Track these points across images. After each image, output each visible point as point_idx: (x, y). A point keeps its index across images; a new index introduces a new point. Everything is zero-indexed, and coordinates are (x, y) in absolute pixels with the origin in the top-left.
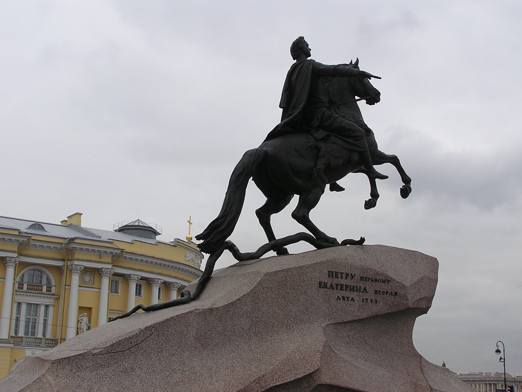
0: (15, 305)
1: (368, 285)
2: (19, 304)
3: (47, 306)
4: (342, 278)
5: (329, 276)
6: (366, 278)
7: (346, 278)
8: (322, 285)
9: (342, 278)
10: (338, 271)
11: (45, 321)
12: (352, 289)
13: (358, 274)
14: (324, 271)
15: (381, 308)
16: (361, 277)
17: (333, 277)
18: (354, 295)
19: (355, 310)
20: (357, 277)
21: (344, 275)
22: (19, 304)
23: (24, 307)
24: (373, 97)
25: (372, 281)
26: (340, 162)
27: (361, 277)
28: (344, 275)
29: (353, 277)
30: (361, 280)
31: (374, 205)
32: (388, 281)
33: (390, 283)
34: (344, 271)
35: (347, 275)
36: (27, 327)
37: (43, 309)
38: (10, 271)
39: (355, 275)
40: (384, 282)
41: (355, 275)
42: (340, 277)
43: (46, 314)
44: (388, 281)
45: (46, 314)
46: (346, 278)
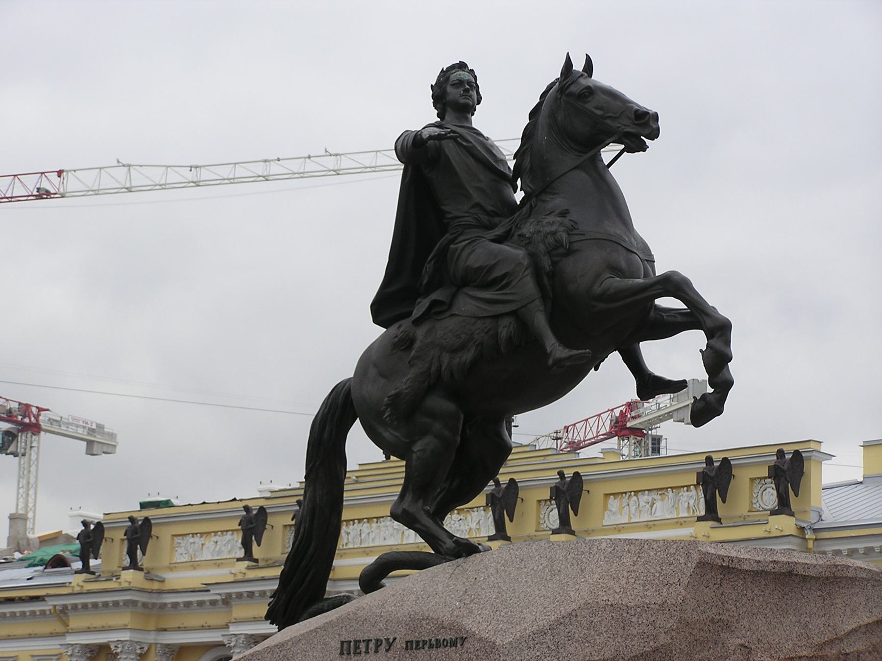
4: (367, 652)
5: (342, 653)
6: (418, 642)
7: (376, 651)
9: (367, 652)
10: (360, 636)
13: (401, 635)
14: (333, 643)
16: (407, 642)
17: (349, 654)
20: (399, 644)
21: (372, 645)
24: (637, 128)
25: (431, 647)
26: (468, 356)
27: (407, 642)
28: (372, 645)
29: (390, 645)
30: (407, 649)
31: (718, 411)
32: (463, 640)
33: (466, 645)
34: (373, 635)
35: (378, 643)
39: (395, 639)
40: (453, 643)
41: (395, 639)
42: (363, 650)
44: (463, 640)
46: (376, 651)
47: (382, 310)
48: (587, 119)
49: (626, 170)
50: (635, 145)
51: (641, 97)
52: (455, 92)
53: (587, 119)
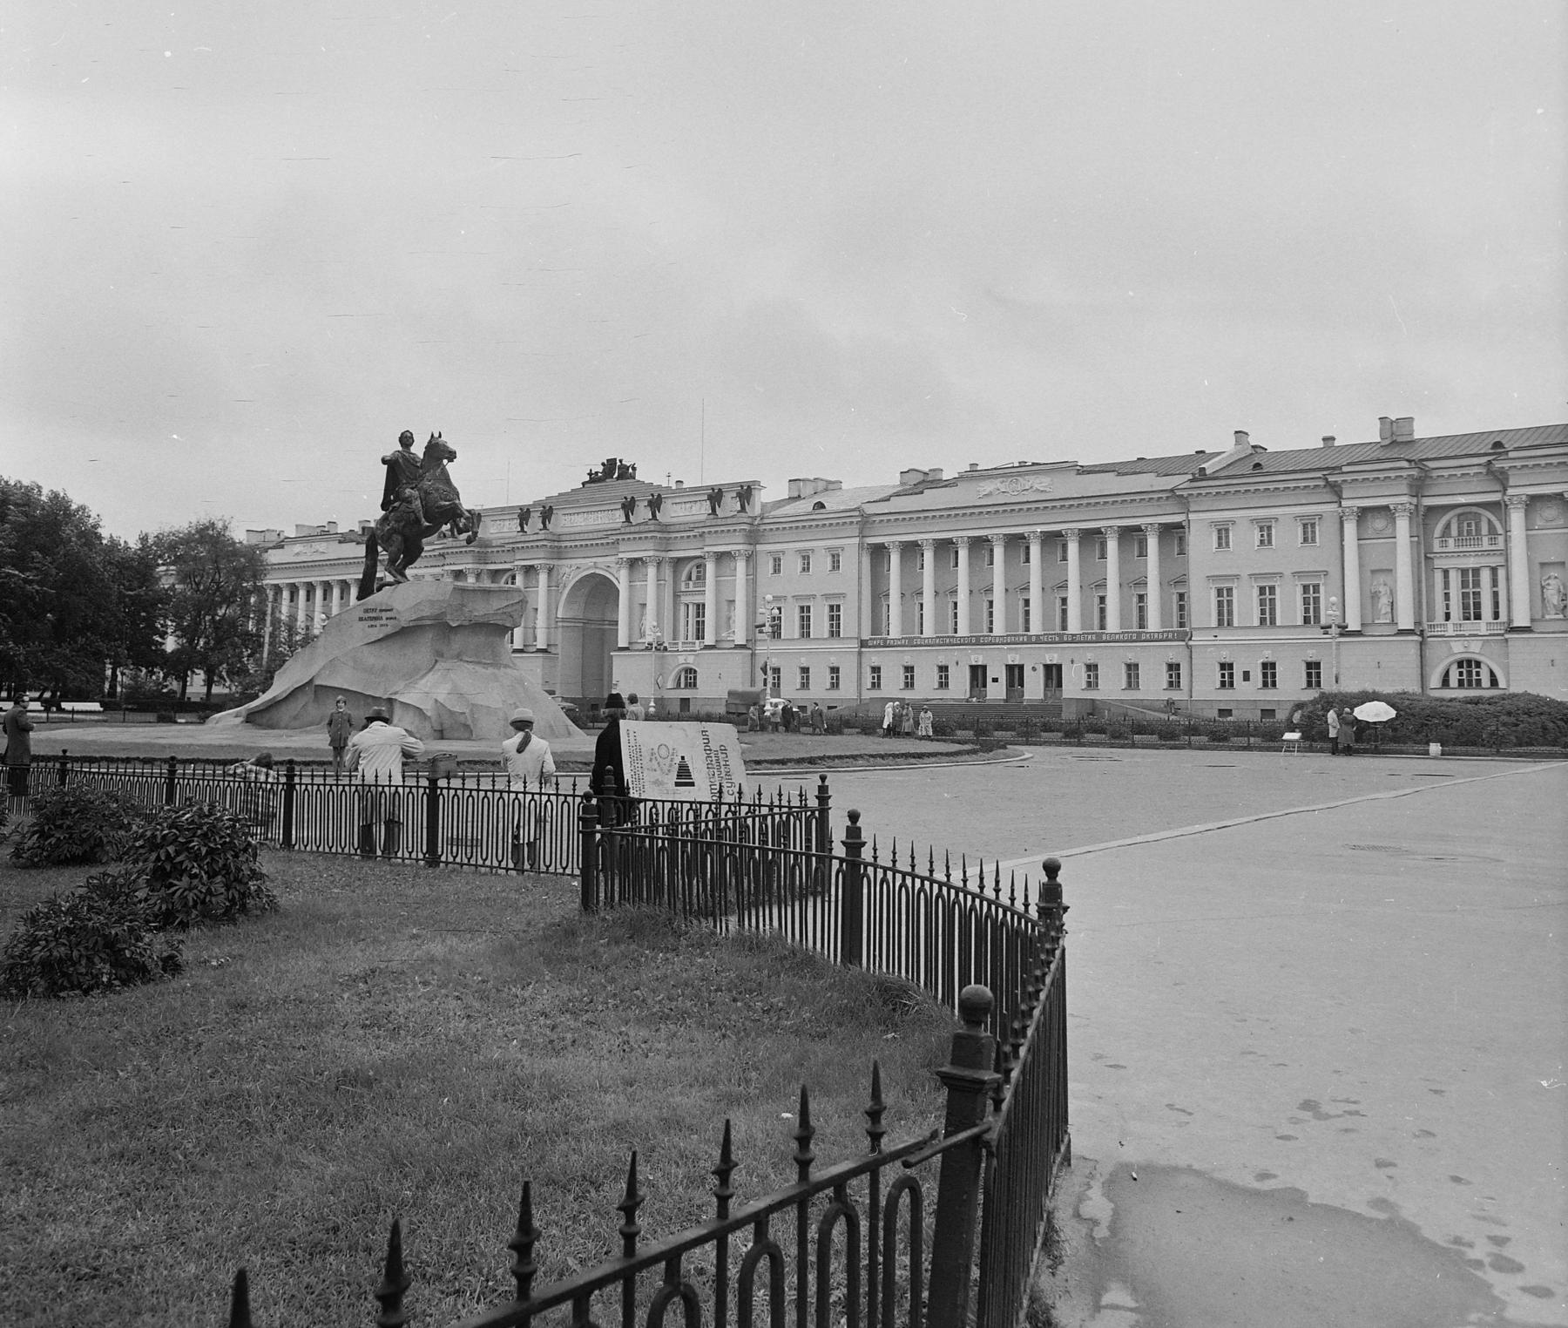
0: (1439, 576)
1: (384, 615)
2: (1446, 572)
3: (1494, 570)
8: (361, 619)
11: (1496, 594)
12: (375, 619)
15: (389, 630)
18: (378, 623)
19: (378, 633)
22: (1446, 572)
23: (1453, 575)
36: (1465, 607)
37: (1485, 576)
38: (1403, 525)
43: (1495, 583)
45: (1495, 583)
47: (384, 506)
48: (439, 452)
49: (450, 467)
50: (451, 460)
51: (452, 446)
52: (406, 440)
53: (439, 452)
